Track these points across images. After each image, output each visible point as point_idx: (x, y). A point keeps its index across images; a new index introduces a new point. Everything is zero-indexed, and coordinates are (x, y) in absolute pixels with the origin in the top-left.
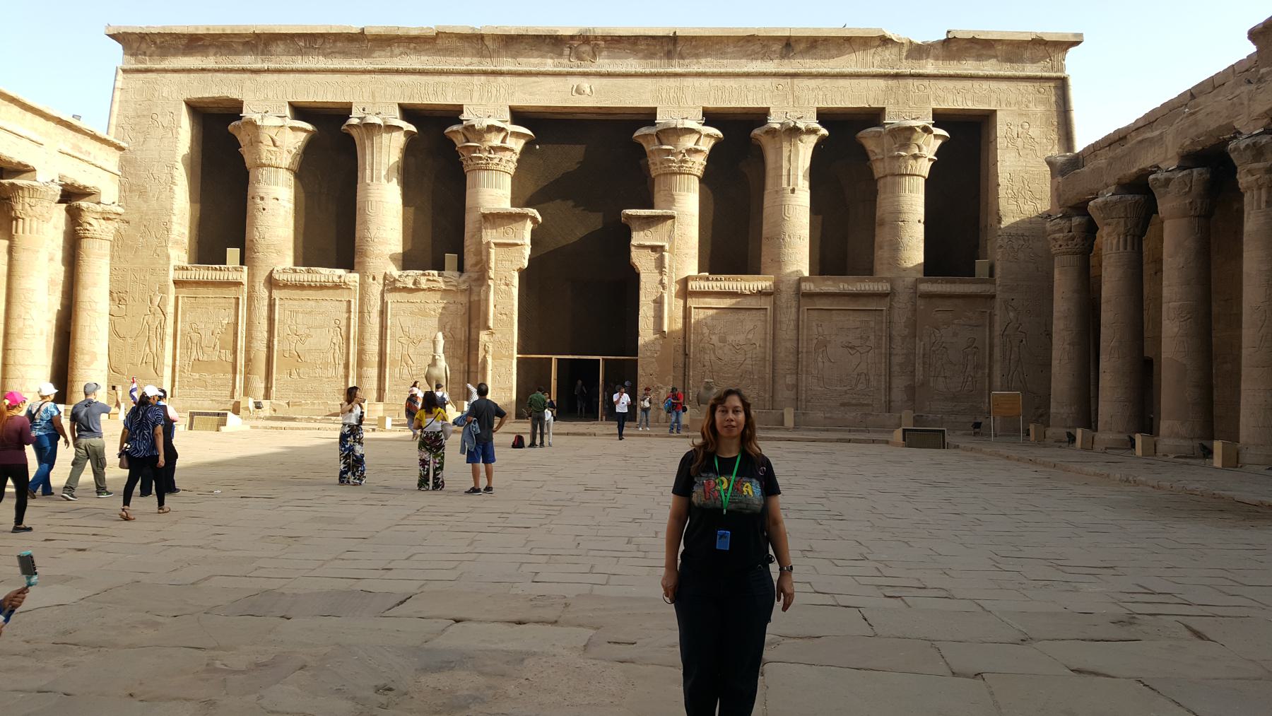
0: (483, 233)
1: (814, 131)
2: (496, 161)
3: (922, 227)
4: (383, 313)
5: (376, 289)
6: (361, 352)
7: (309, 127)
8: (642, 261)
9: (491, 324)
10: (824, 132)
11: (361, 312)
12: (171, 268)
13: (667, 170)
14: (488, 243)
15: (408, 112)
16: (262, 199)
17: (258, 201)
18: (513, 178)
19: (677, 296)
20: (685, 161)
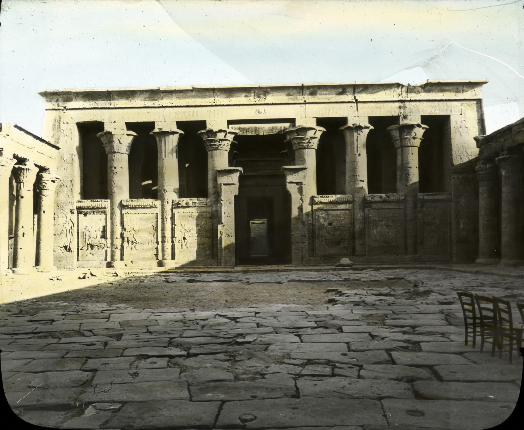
0: (218, 180)
1: (366, 128)
2: (222, 146)
3: (418, 169)
4: (173, 218)
5: (168, 207)
6: (163, 237)
7: (135, 134)
8: (292, 189)
9: (223, 221)
10: (372, 127)
11: (163, 218)
12: (75, 202)
13: (302, 147)
14: (221, 184)
15: (180, 124)
16: (115, 168)
17: (113, 169)
18: (229, 153)
19: (309, 204)
20: (310, 143)
